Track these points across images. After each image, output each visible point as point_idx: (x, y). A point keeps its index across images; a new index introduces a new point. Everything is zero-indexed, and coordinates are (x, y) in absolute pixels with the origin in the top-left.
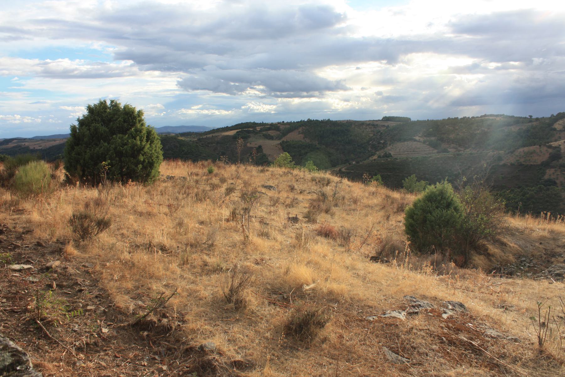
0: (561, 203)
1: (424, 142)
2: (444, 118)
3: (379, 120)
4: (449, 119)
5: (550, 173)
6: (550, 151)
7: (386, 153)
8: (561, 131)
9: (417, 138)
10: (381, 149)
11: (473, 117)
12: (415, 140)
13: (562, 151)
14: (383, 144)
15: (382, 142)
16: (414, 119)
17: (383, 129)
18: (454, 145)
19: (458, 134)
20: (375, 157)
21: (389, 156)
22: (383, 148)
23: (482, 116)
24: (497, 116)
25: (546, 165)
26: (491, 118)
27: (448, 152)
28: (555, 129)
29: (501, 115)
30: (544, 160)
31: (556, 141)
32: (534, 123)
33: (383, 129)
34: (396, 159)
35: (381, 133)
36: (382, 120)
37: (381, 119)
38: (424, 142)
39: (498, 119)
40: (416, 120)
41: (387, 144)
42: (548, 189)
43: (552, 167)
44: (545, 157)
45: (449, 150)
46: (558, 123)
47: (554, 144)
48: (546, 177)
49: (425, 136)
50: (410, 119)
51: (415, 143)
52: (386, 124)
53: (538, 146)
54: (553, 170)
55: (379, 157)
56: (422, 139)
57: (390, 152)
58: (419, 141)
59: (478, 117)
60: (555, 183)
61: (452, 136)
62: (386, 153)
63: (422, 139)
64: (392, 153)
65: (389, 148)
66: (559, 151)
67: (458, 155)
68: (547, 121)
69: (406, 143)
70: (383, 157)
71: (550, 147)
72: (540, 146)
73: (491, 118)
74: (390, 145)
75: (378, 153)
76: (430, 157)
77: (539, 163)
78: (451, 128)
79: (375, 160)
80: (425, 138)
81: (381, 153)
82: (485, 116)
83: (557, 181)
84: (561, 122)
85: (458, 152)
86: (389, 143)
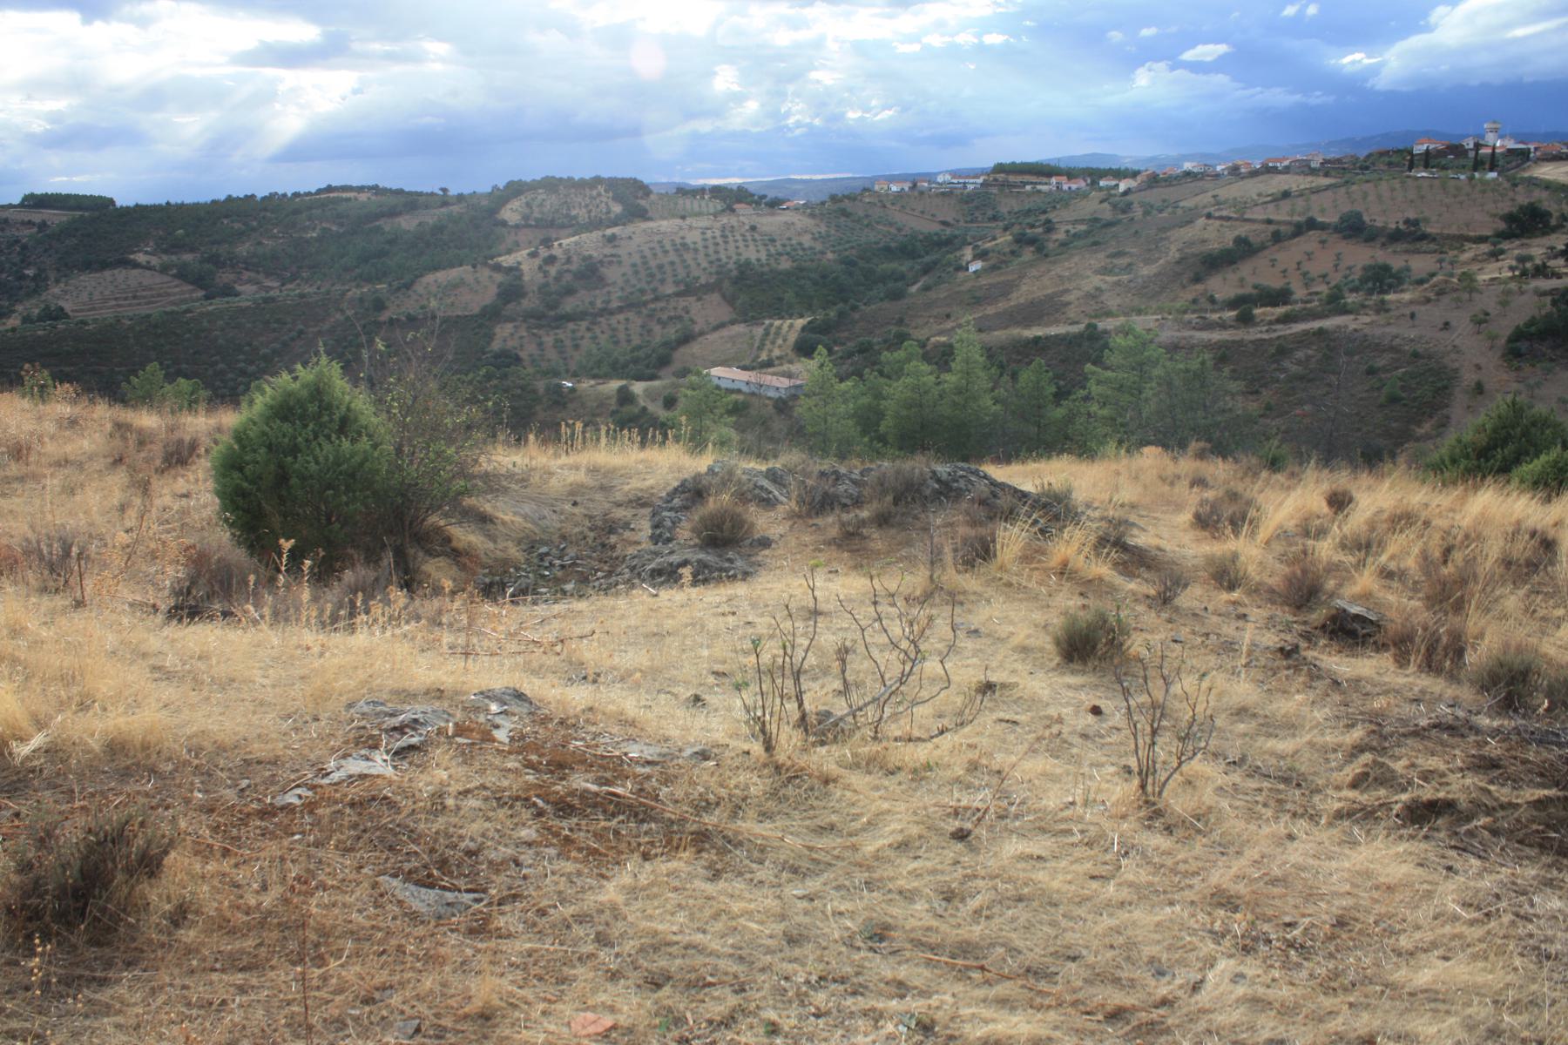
0: (538, 408)
1: (164, 269)
2: (216, 197)
3: (11, 206)
4: (229, 199)
5: (504, 335)
6: (499, 277)
7: (47, 307)
8: (517, 226)
9: (141, 258)
10: (29, 295)
11: (296, 195)
12: (136, 265)
13: (526, 278)
14: (34, 279)
15: (30, 272)
16: (123, 200)
17: (27, 232)
18: (253, 275)
19: (260, 243)
20: (14, 321)
21: (60, 314)
22: (36, 292)
23: (319, 191)
24: (361, 189)
25: (492, 315)
26: (345, 195)
27: (237, 295)
28: (504, 224)
29: (370, 188)
30: (488, 301)
31: (509, 252)
32: (455, 209)
33: (27, 232)
34: (84, 323)
35: (24, 247)
36: (22, 205)
37: (16, 201)
38: (164, 269)
39: (363, 197)
40: (131, 204)
41: (46, 279)
42: (505, 376)
43: (510, 320)
44: (489, 296)
45: (238, 288)
46: (509, 206)
47: (507, 261)
48: (496, 345)
49: (165, 252)
50: (111, 201)
51: (135, 272)
52: (37, 216)
53: (469, 268)
54: (509, 327)
55: (27, 319)
56: (155, 261)
57: (61, 303)
58: (148, 267)
59: (309, 194)
60: (518, 359)
61: (243, 249)
62: (47, 307)
63: (155, 261)
64: (68, 306)
65: (56, 290)
66: (520, 277)
67: (266, 300)
68: (484, 203)
69: (107, 274)
70: (40, 319)
71: (498, 268)
72: (474, 266)
73: (345, 195)
74: (57, 281)
75: (19, 308)
76: (188, 311)
77: (476, 310)
78: (237, 226)
79: (14, 330)
80: (165, 258)
81: (33, 307)
82: (330, 189)
83: (523, 355)
84: (516, 204)
85: (263, 294)
86: (52, 275)
